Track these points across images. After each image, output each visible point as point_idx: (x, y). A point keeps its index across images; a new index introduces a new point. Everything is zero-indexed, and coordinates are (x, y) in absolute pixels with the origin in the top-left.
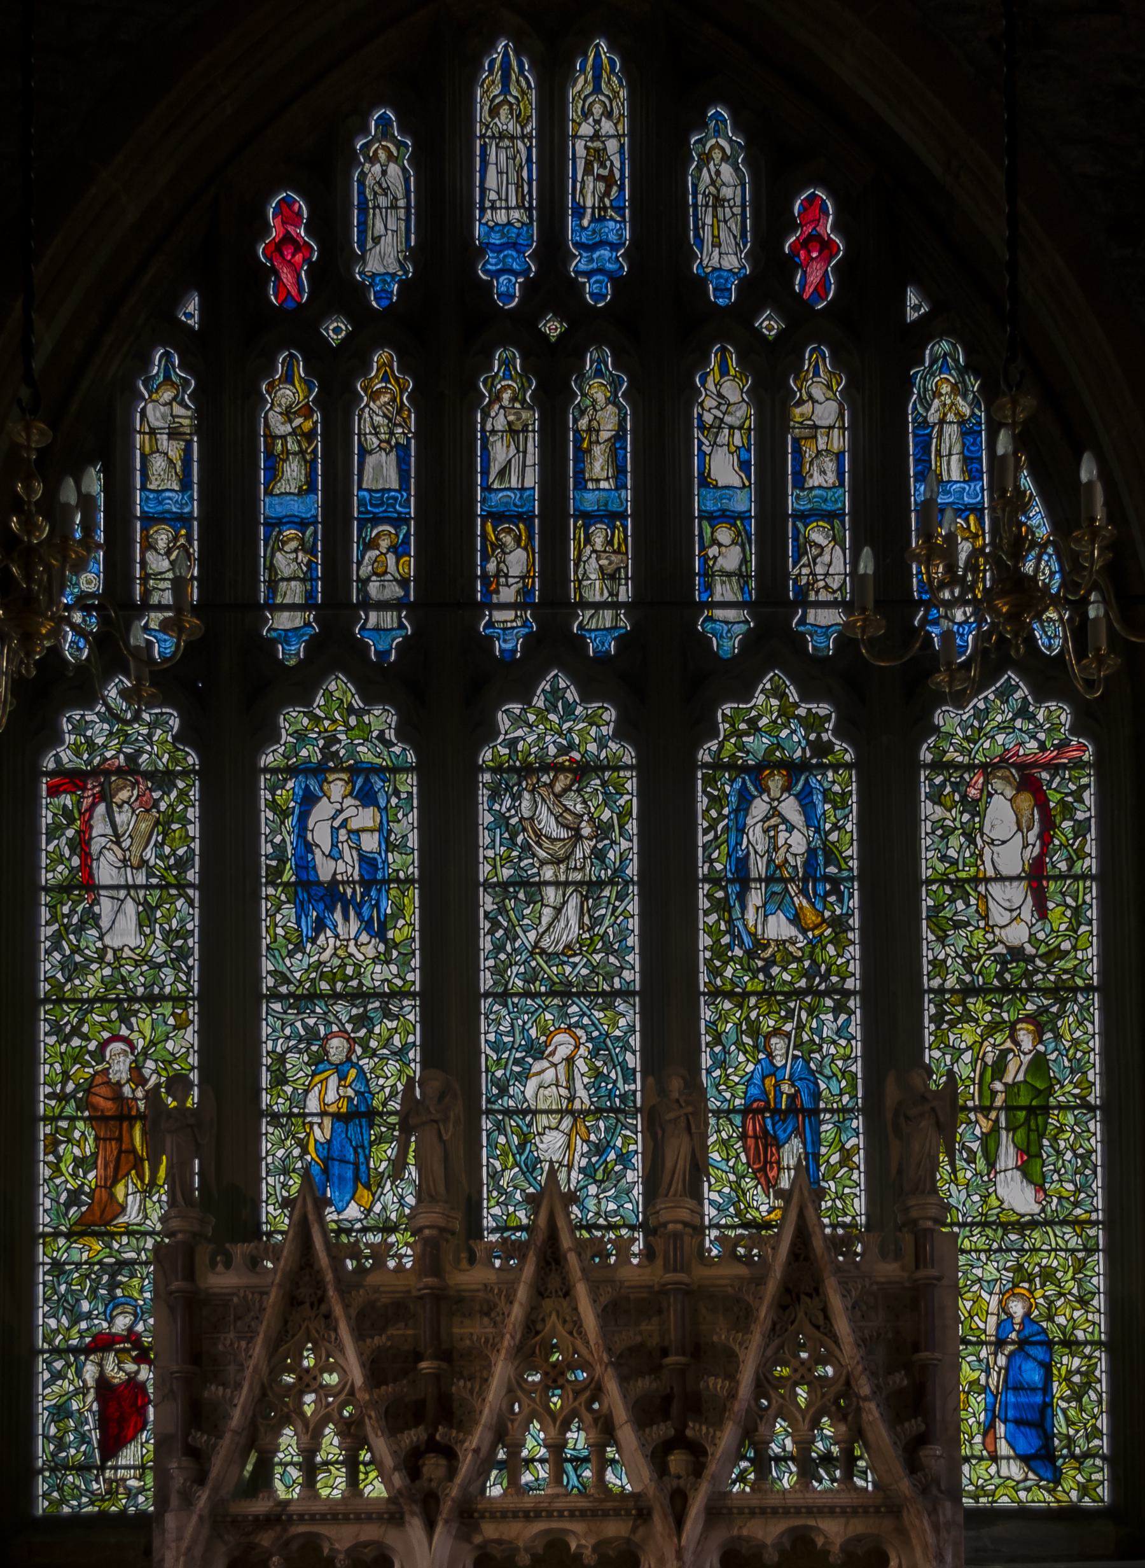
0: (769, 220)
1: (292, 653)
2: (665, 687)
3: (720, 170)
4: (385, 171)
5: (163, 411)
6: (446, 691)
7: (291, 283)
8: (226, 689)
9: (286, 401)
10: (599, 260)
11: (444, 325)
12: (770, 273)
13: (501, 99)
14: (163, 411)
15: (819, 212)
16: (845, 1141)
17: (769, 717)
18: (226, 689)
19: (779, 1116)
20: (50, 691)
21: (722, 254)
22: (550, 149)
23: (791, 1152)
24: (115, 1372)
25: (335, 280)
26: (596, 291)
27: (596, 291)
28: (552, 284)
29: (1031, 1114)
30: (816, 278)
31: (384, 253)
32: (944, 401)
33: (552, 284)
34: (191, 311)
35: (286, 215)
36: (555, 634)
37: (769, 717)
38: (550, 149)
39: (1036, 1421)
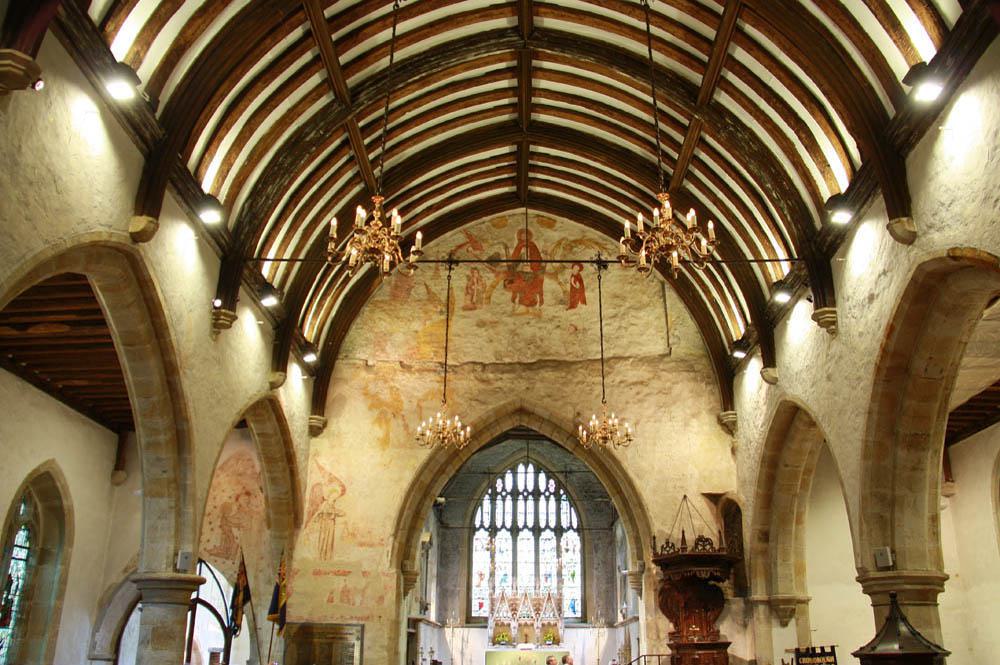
0: (548, 483)
1: (499, 527)
2: (537, 531)
3: (542, 477)
4: (509, 477)
5: (487, 503)
6: (515, 531)
7: (499, 490)
8: (493, 530)
9: (499, 503)
10: (530, 488)
11: (515, 494)
12: (547, 489)
13: (521, 468)
14: (487, 503)
15: (552, 482)
16: (554, 579)
17: (548, 534)
18: (493, 530)
19: (548, 576)
20: (474, 530)
21: (542, 488)
22: (526, 477)
23: (549, 579)
24: (481, 601)
25: (504, 489)
26: (530, 490)
27: (530, 490)
28: (526, 490)
29: (573, 576)
30: (552, 490)
31: (509, 487)
32: (565, 505)
33: (526, 490)
34: (490, 491)
35: (499, 481)
36: (525, 526)
37: (548, 534)
38: (526, 477)
39: (573, 608)
